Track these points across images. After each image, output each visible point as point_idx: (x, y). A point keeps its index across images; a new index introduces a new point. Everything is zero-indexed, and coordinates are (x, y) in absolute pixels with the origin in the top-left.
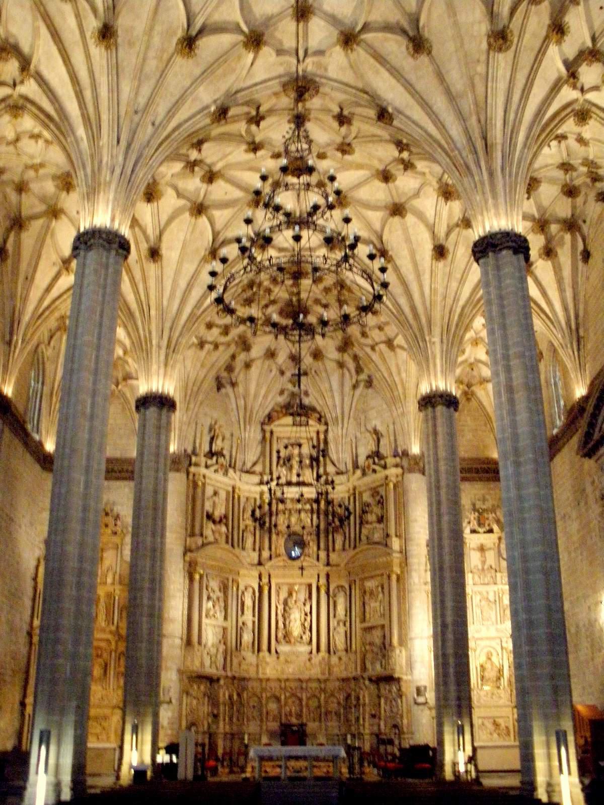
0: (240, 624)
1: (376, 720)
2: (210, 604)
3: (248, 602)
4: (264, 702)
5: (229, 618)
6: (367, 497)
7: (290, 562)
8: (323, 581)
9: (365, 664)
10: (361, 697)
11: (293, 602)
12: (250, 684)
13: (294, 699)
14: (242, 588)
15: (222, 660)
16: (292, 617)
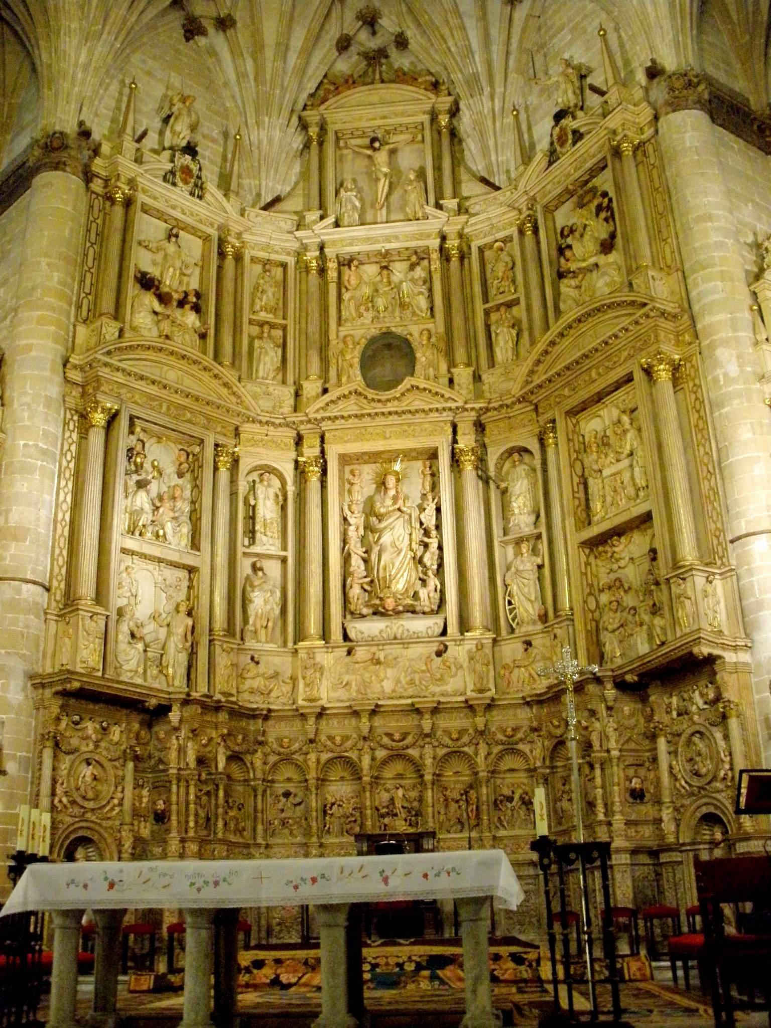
0: (244, 567)
1: (646, 810)
2: (142, 499)
3: (267, 510)
4: (312, 775)
5: (205, 544)
6: (564, 216)
7: (371, 394)
8: (466, 441)
9: (599, 644)
10: (595, 739)
11: (389, 502)
12: (275, 731)
13: (398, 767)
14: (244, 467)
15: (183, 658)
16: (386, 539)
